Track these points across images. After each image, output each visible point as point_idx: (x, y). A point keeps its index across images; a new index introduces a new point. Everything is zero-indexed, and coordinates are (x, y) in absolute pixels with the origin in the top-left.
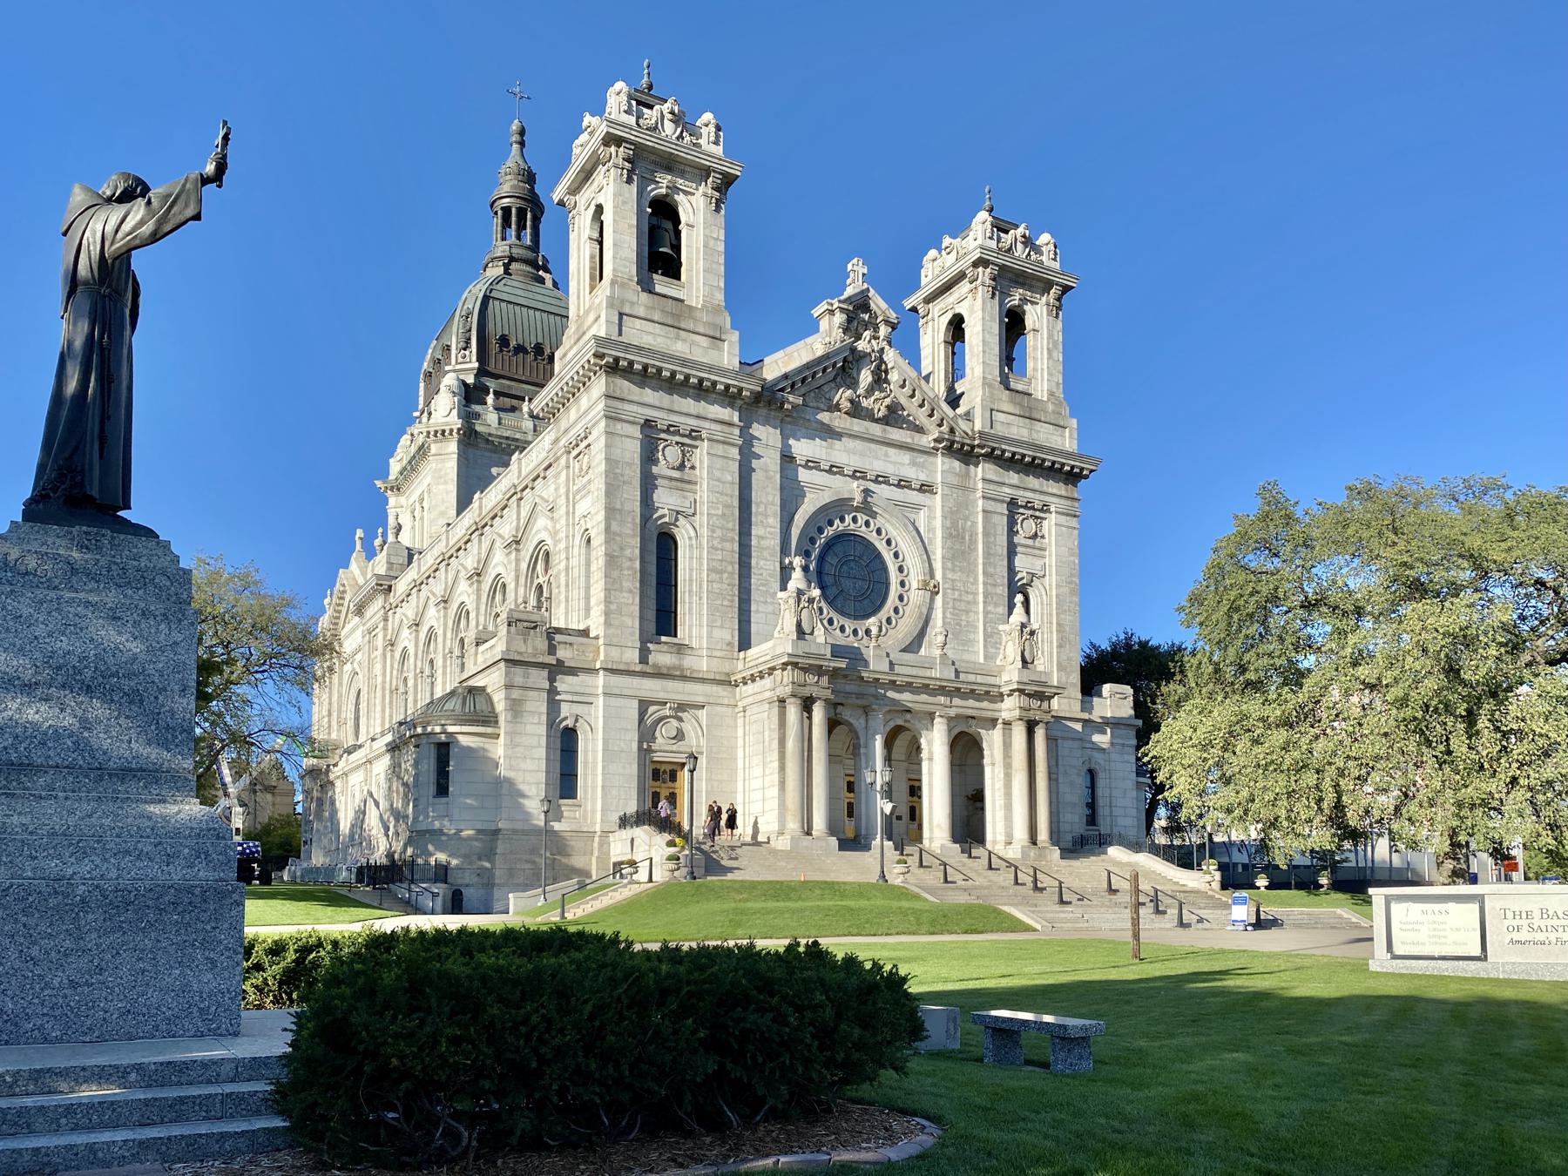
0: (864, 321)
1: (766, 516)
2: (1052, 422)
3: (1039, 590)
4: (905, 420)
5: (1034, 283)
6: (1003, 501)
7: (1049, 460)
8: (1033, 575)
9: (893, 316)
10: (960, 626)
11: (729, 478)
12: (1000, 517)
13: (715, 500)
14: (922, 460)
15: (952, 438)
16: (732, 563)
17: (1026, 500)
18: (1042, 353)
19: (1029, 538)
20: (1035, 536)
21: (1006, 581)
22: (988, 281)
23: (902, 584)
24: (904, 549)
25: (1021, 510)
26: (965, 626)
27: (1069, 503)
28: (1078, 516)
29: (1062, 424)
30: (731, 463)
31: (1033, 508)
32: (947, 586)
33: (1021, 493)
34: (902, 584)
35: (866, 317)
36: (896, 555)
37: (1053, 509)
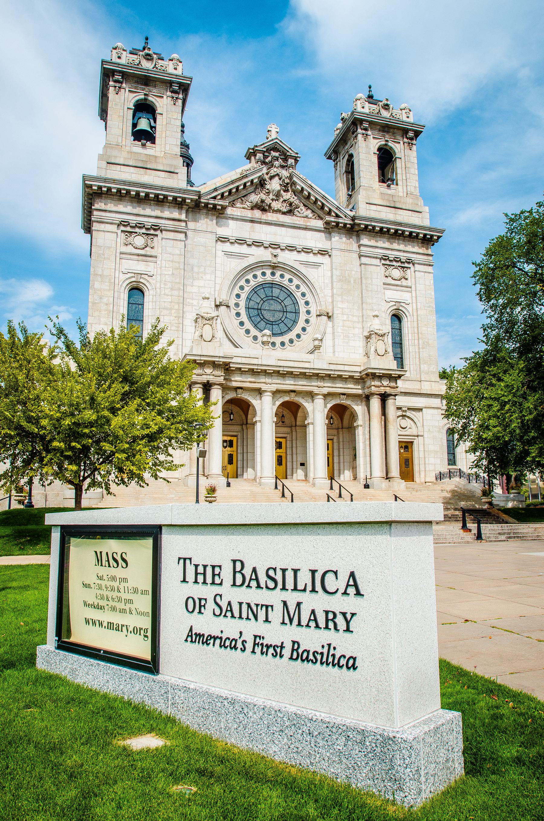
1: (205, 273)
2: (411, 209)
6: (377, 258)
7: (407, 231)
10: (349, 337)
11: (178, 252)
13: (167, 266)
15: (337, 220)
16: (178, 303)
17: (394, 256)
23: (308, 312)
26: (352, 337)
27: (425, 257)
28: (432, 265)
29: (418, 210)
30: (179, 243)
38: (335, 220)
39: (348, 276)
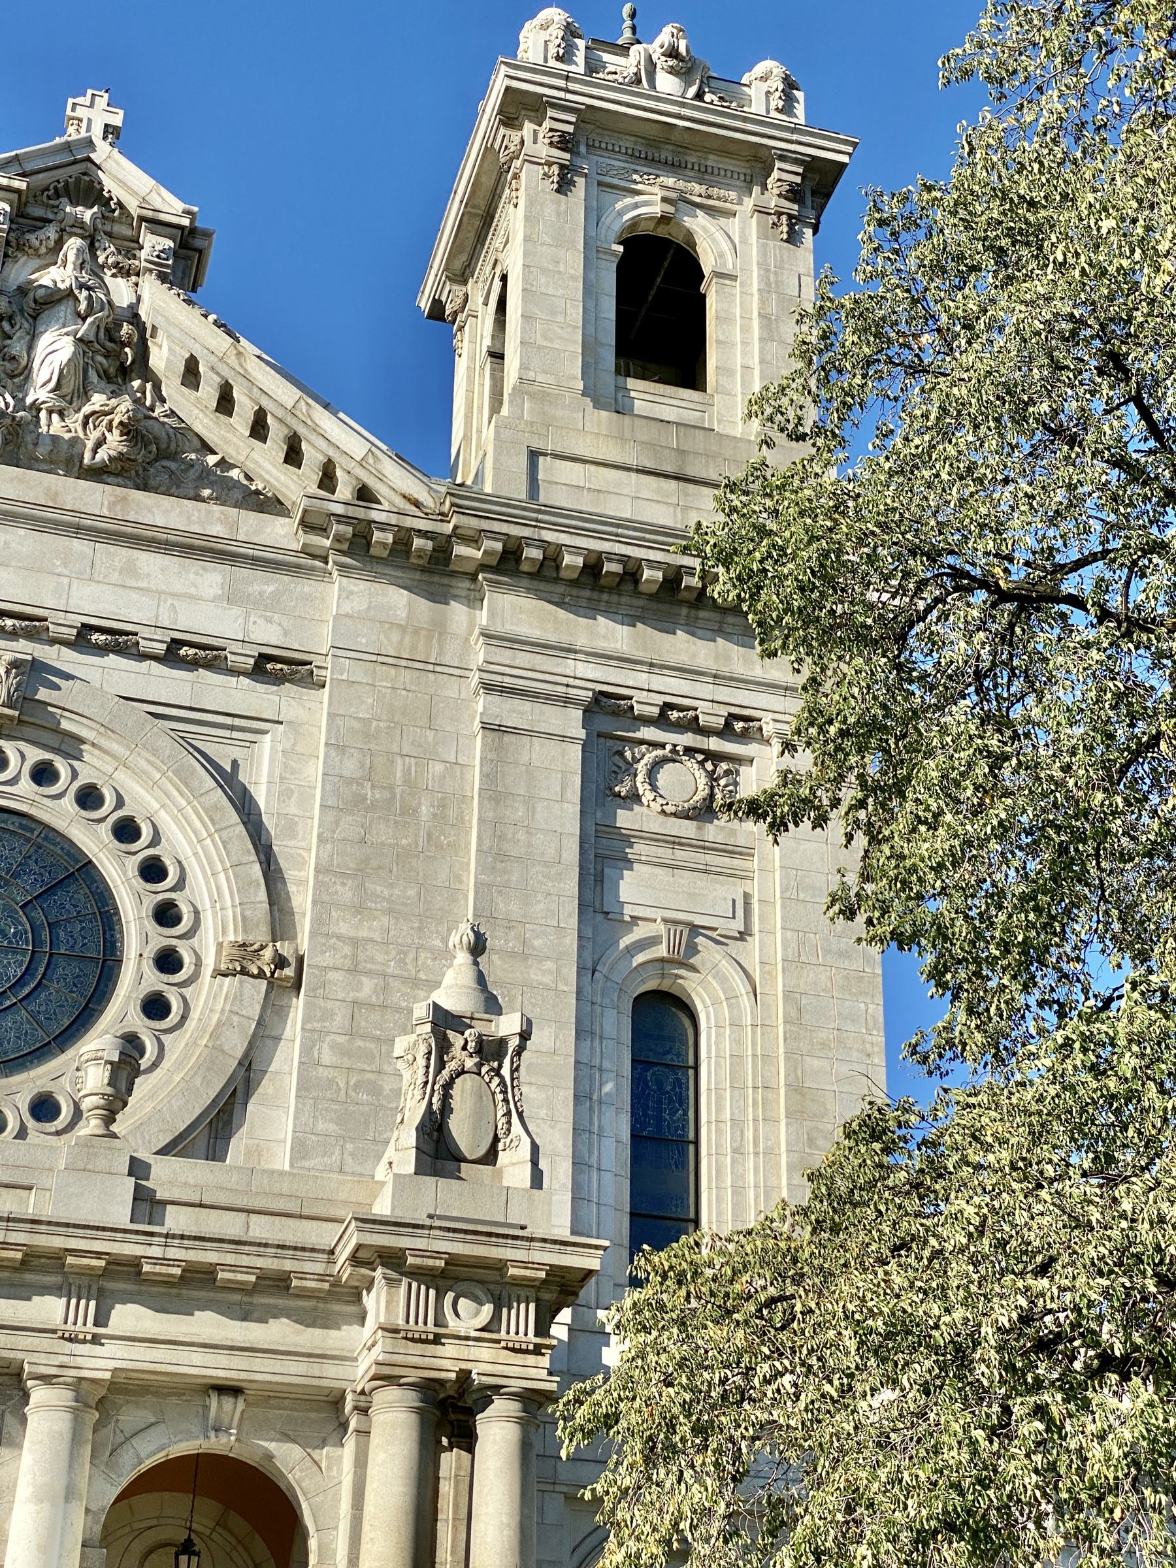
0: (79, 223)
3: (723, 980)
4: (205, 476)
5: (712, 161)
6: (566, 701)
8: (695, 929)
9: (172, 207)
12: (553, 747)
14: (271, 589)
15: (360, 513)
17: (660, 700)
18: (746, 329)
19: (685, 815)
20: (705, 811)
21: (571, 942)
22: (544, 151)
23: (167, 961)
24: (185, 851)
25: (649, 733)
31: (694, 726)
32: (327, 959)
33: (640, 678)
34: (167, 961)
35: (87, 215)
36: (152, 871)
37: (768, 728)
38: (351, 511)
39: (407, 781)
